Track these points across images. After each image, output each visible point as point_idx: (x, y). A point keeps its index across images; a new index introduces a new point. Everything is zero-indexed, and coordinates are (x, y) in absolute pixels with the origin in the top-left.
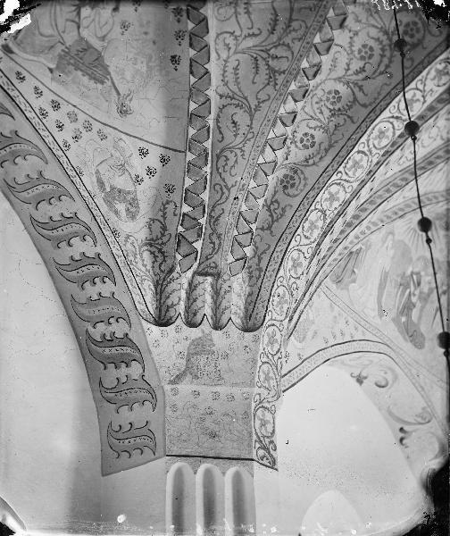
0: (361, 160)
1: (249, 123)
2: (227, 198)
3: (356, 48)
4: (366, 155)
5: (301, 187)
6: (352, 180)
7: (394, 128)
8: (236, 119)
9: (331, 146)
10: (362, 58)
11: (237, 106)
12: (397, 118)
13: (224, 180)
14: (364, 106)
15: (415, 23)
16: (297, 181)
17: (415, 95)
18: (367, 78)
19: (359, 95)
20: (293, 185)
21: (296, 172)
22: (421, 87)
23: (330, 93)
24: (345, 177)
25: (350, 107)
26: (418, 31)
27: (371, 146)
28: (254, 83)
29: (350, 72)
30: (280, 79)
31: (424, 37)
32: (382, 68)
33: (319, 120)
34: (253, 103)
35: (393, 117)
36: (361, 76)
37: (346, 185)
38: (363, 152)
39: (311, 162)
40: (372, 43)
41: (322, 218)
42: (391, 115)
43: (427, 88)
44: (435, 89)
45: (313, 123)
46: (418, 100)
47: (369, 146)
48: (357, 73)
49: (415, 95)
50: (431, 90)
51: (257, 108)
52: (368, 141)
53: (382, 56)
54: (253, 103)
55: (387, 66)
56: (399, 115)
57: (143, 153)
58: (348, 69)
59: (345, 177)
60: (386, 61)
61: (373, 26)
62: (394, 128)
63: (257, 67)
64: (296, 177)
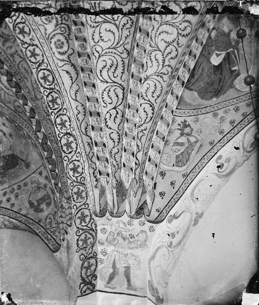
0: (53, 97)
4: (51, 93)
6: (61, 107)
7: (44, 69)
12: (39, 66)
17: (30, 51)
24: (56, 111)
27: (48, 87)
35: (37, 68)
37: (61, 112)
38: (49, 94)
41: (69, 136)
42: (36, 69)
43: (29, 41)
44: (31, 37)
46: (34, 49)
47: (48, 89)
49: (30, 51)
50: (30, 40)
52: (44, 88)
56: (38, 64)
57: (41, 173)
59: (56, 111)
62: (44, 69)
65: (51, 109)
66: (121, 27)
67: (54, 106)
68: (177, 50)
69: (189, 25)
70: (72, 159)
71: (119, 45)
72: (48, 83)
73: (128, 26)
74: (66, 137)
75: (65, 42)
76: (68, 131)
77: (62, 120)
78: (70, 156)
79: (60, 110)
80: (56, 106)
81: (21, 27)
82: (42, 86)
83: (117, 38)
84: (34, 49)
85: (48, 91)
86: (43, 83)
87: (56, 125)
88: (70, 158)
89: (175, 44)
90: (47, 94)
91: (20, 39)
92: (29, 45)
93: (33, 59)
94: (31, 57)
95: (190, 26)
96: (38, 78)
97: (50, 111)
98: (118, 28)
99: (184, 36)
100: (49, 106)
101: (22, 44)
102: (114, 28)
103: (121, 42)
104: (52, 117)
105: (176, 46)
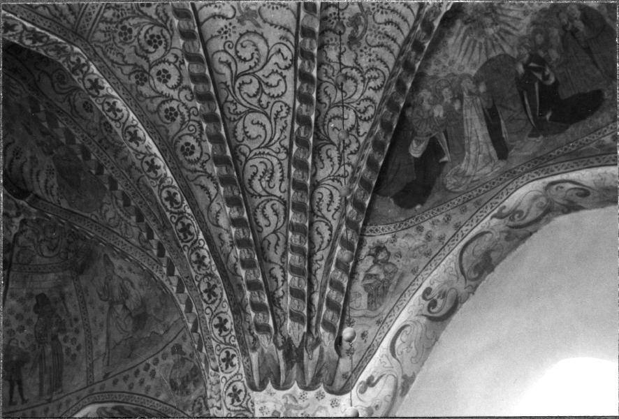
0: (183, 224)
6: (195, 238)
17: (147, 162)
22: (142, 156)
24: (189, 244)
27: (176, 211)
35: (159, 186)
41: (210, 278)
42: (157, 187)
43: (144, 151)
47: (176, 213)
49: (147, 162)
52: (171, 212)
59: (189, 244)
65: (182, 242)
66: (273, 116)
67: (186, 237)
68: (358, 141)
69: (371, 103)
70: (217, 311)
71: (273, 141)
72: (175, 206)
73: (283, 114)
74: (206, 279)
75: (196, 144)
76: (208, 272)
77: (198, 255)
78: (213, 307)
79: (195, 242)
80: (189, 237)
81: (132, 132)
82: (168, 210)
83: (269, 133)
84: (152, 160)
85: (177, 216)
86: (169, 207)
87: (191, 264)
88: (213, 310)
89: (354, 132)
90: (175, 221)
91: (132, 148)
92: (145, 155)
93: (152, 174)
94: (149, 171)
95: (373, 105)
96: (161, 200)
97: (182, 245)
98: (269, 119)
99: (365, 120)
100: (180, 237)
101: (136, 155)
102: (264, 120)
103: (276, 138)
104: (185, 253)
105: (356, 135)
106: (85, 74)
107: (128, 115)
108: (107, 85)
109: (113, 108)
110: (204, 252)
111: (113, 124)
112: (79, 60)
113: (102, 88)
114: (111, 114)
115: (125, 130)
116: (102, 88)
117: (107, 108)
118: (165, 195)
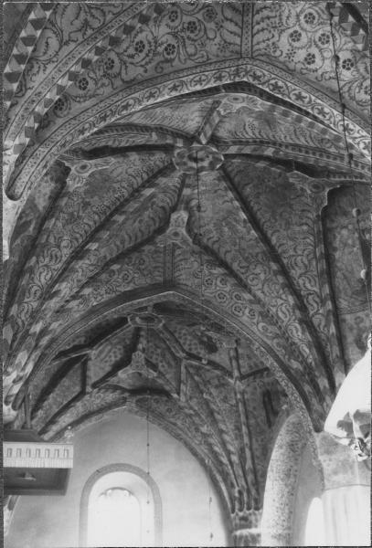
1: (57, 50)
2: (23, 95)
3: (136, 40)
5: (65, 113)
8: (49, 41)
9: (94, 96)
10: (136, 49)
11: (55, 33)
13: (25, 80)
14: (122, 80)
15: (174, 47)
16: (64, 107)
18: (132, 63)
19: (123, 71)
20: (61, 109)
21: (66, 101)
23: (109, 59)
25: (115, 77)
26: (173, 53)
28: (72, 24)
29: (126, 54)
30: (89, 32)
31: (174, 59)
32: (143, 63)
33: (95, 73)
34: (66, 38)
36: (130, 60)
39: (78, 99)
40: (145, 43)
45: (92, 75)
48: (129, 56)
51: (67, 43)
53: (147, 55)
54: (66, 38)
55: (147, 64)
58: (126, 51)
60: (147, 59)
61: (152, 33)
63: (78, 15)
64: (65, 104)
93: (148, 94)
104: (91, 119)
106: (230, 76)
107: (188, 89)
108: (215, 85)
109: (200, 81)
110: (87, 134)
111: (191, 77)
112: (239, 76)
113: (215, 81)
114: (197, 78)
115: (183, 83)
116: (215, 81)
117: (203, 78)
118: (131, 102)
